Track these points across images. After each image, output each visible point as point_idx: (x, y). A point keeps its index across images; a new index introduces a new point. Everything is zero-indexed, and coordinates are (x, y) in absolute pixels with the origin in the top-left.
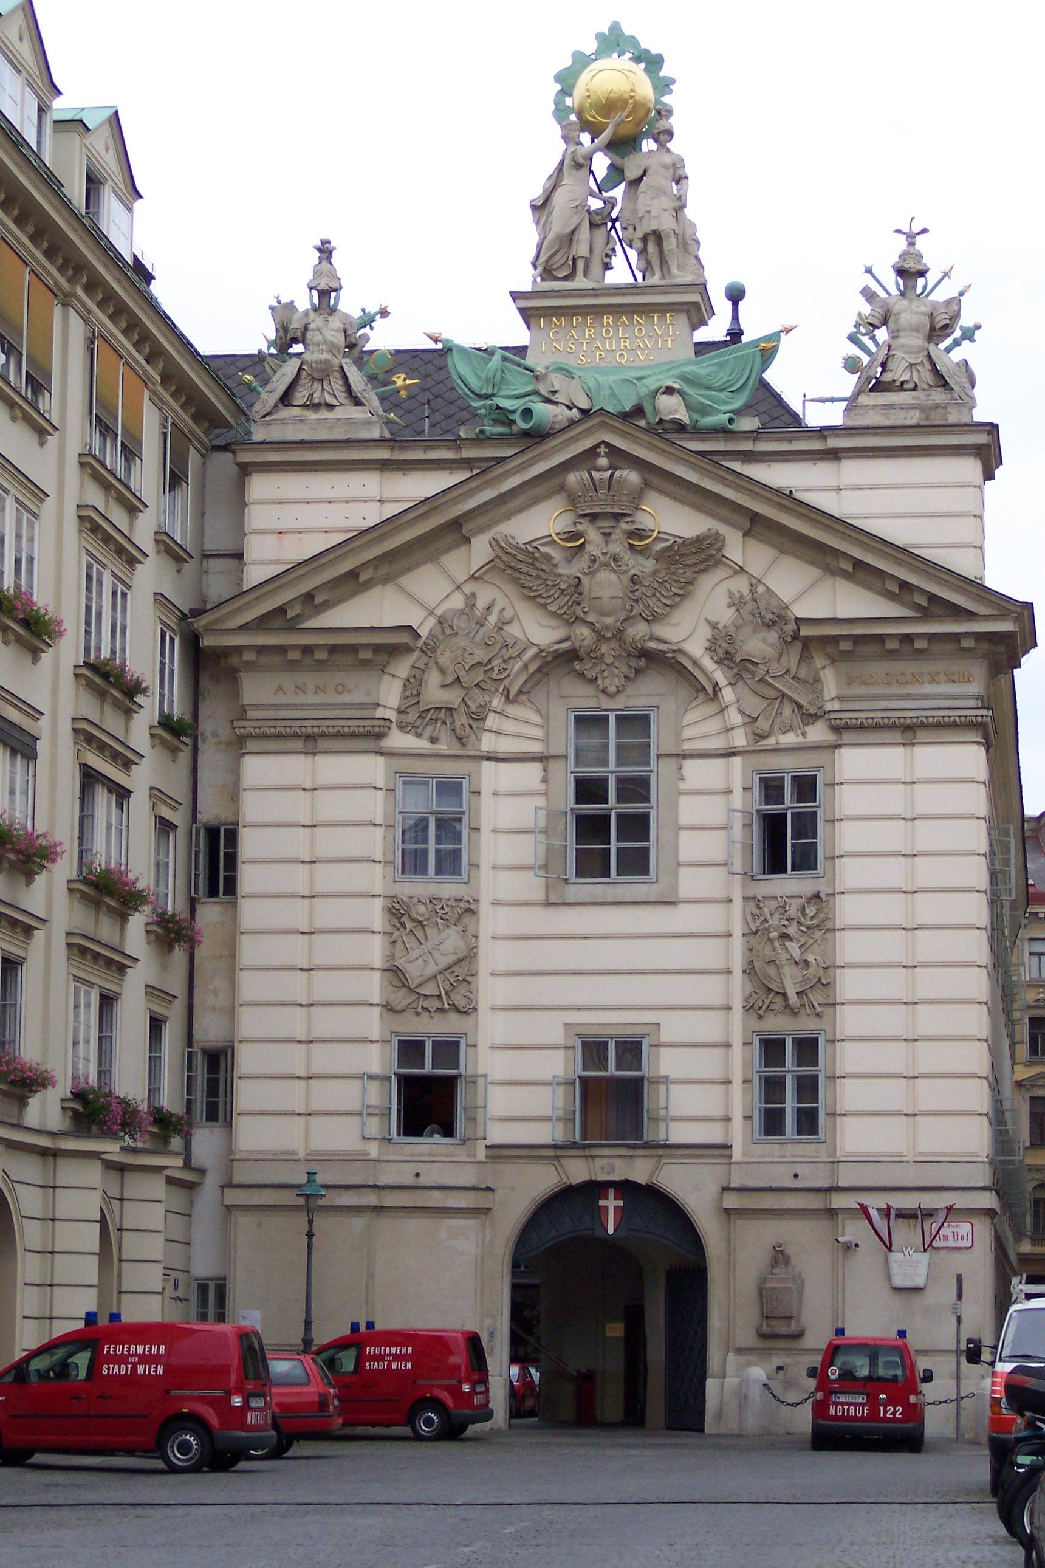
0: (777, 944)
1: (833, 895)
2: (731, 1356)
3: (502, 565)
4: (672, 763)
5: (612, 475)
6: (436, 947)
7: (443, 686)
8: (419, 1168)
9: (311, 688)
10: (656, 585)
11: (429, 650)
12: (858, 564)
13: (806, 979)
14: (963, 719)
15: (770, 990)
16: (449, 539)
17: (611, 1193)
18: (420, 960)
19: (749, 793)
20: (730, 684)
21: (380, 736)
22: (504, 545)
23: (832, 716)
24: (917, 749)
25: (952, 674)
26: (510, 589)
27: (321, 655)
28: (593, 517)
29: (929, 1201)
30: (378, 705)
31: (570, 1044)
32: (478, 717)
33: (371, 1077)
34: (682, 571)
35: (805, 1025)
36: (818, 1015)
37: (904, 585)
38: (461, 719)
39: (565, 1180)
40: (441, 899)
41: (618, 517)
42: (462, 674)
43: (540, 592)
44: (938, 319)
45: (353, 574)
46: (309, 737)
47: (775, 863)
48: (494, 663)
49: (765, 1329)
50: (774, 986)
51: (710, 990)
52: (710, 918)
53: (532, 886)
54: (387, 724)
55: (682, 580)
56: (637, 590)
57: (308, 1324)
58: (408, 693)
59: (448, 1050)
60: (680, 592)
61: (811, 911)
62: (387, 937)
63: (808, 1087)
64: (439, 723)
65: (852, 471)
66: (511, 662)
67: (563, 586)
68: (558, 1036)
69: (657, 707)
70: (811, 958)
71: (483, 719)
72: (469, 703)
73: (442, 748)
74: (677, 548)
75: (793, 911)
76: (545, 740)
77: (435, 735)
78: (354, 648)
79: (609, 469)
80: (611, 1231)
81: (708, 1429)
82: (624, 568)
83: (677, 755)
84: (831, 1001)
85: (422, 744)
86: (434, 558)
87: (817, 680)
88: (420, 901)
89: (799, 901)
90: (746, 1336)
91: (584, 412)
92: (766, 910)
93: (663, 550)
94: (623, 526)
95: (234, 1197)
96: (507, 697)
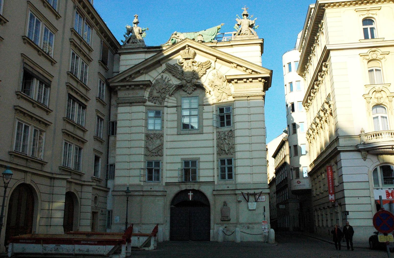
0: (223, 141)
1: (234, 130)
6: (155, 143)
8: (152, 187)
11: (154, 86)
12: (238, 65)
13: (229, 147)
15: (222, 150)
16: (158, 65)
19: (217, 112)
21: (145, 102)
26: (170, 74)
27: (133, 87)
30: (144, 96)
31: (182, 162)
32: (164, 99)
33: (142, 169)
35: (229, 156)
36: (232, 154)
37: (247, 69)
39: (181, 189)
41: (189, 59)
45: (139, 71)
46: (131, 103)
47: (222, 125)
48: (167, 88)
49: (222, 219)
50: (223, 149)
51: (210, 151)
52: (210, 136)
53: (175, 131)
59: (158, 164)
61: (230, 134)
63: (230, 169)
66: (170, 88)
67: (180, 73)
68: (180, 161)
70: (230, 143)
71: (165, 99)
73: (156, 105)
75: (226, 133)
76: (177, 103)
78: (138, 85)
80: (190, 200)
81: (211, 240)
83: (203, 105)
84: (234, 151)
85: (153, 104)
86: (155, 69)
90: (219, 221)
94: (191, 60)
95: (115, 193)
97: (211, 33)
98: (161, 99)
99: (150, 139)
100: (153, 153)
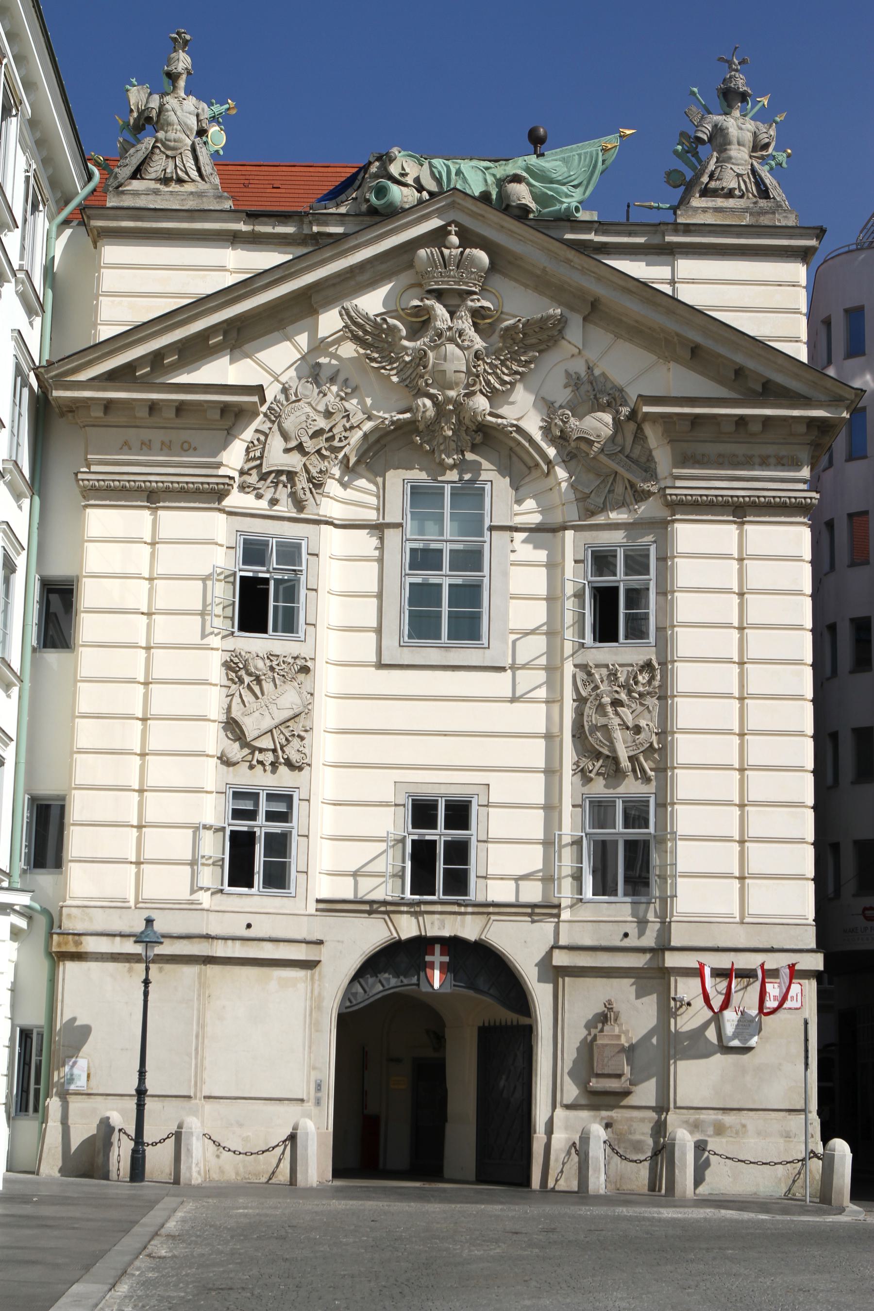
0: (609, 709)
2: (560, 1112)
3: (350, 335)
4: (507, 534)
5: (462, 253)
7: (287, 451)
9: (157, 445)
10: (497, 362)
14: (793, 500)
15: (598, 755)
17: (437, 948)
18: (257, 714)
20: (564, 461)
22: (353, 314)
23: (668, 491)
24: (746, 527)
25: (782, 458)
28: (439, 295)
29: (772, 961)
32: (317, 485)
34: (523, 350)
37: (739, 372)
38: (302, 482)
40: (278, 656)
42: (305, 439)
43: (384, 364)
44: (761, 137)
48: (335, 431)
54: (232, 482)
55: (523, 358)
56: (479, 366)
57: (142, 1073)
58: (252, 455)
60: (520, 369)
61: (643, 678)
62: (224, 689)
64: (281, 486)
65: (686, 267)
69: (491, 481)
70: (643, 723)
72: (310, 467)
74: (521, 326)
76: (381, 509)
77: (277, 496)
79: (458, 247)
80: (437, 985)
82: (466, 343)
85: (262, 505)
87: (650, 458)
88: (257, 656)
89: (630, 669)
91: (431, 194)
92: (597, 676)
93: (507, 329)
96: (347, 466)
97: (566, 175)
98: (307, 485)
99: (247, 679)
100: (261, 750)
